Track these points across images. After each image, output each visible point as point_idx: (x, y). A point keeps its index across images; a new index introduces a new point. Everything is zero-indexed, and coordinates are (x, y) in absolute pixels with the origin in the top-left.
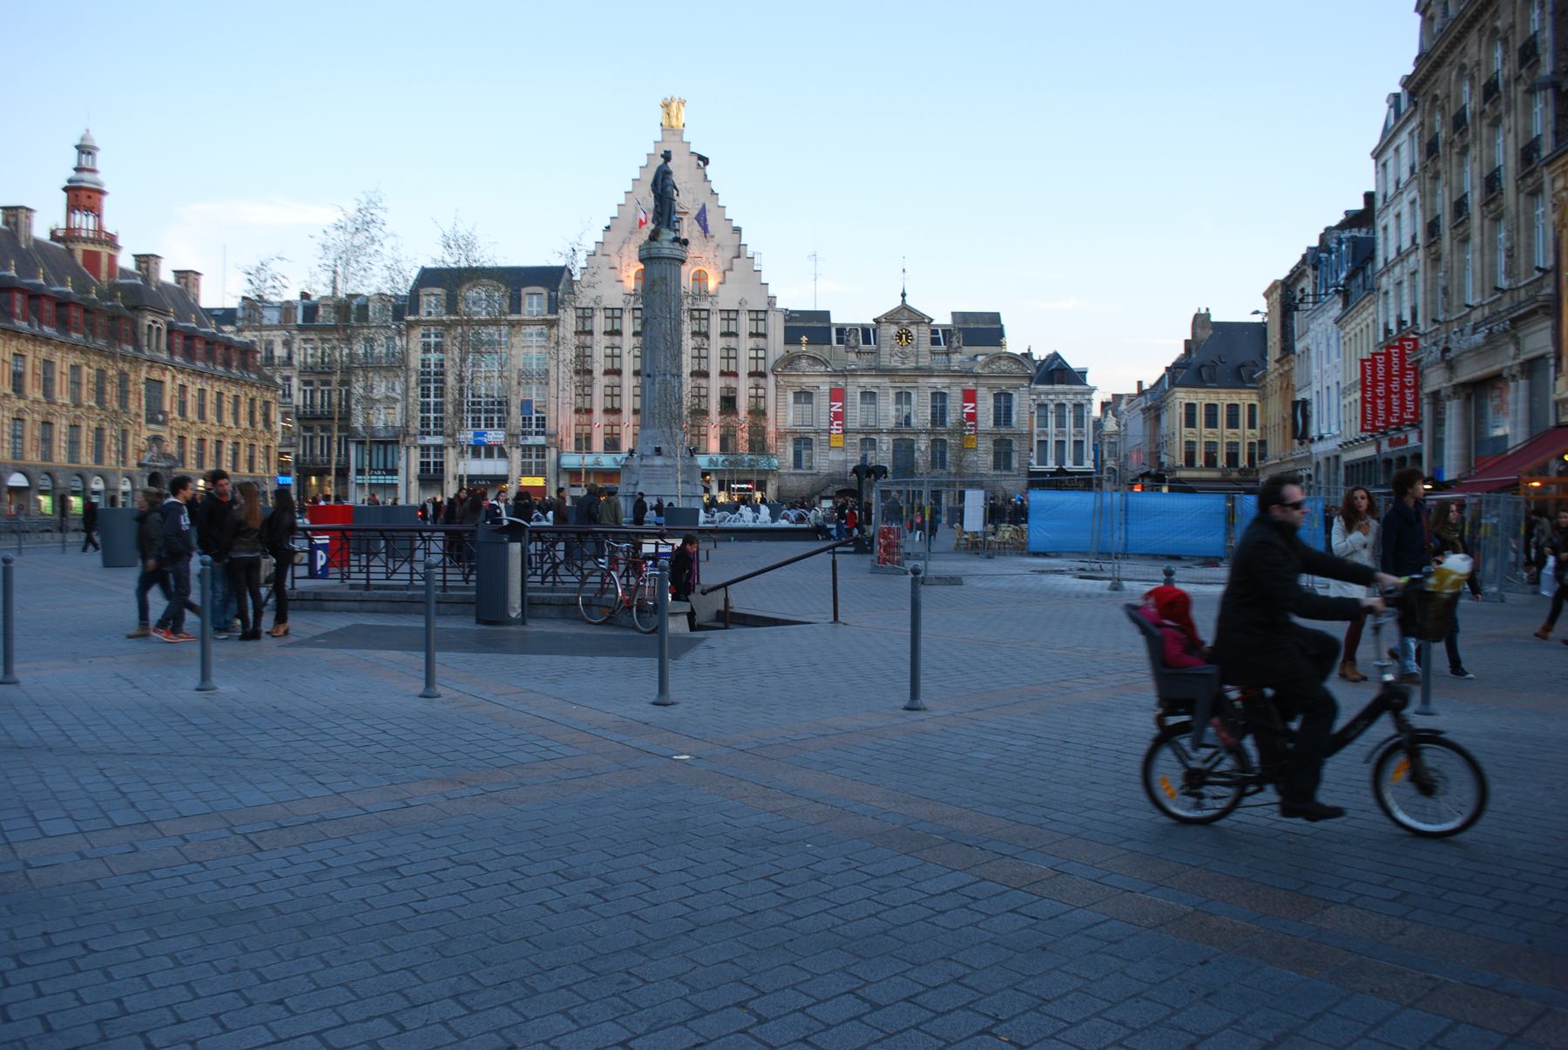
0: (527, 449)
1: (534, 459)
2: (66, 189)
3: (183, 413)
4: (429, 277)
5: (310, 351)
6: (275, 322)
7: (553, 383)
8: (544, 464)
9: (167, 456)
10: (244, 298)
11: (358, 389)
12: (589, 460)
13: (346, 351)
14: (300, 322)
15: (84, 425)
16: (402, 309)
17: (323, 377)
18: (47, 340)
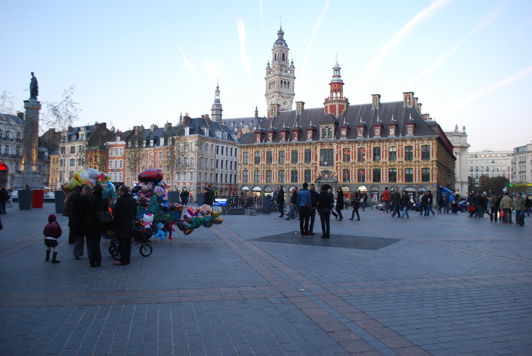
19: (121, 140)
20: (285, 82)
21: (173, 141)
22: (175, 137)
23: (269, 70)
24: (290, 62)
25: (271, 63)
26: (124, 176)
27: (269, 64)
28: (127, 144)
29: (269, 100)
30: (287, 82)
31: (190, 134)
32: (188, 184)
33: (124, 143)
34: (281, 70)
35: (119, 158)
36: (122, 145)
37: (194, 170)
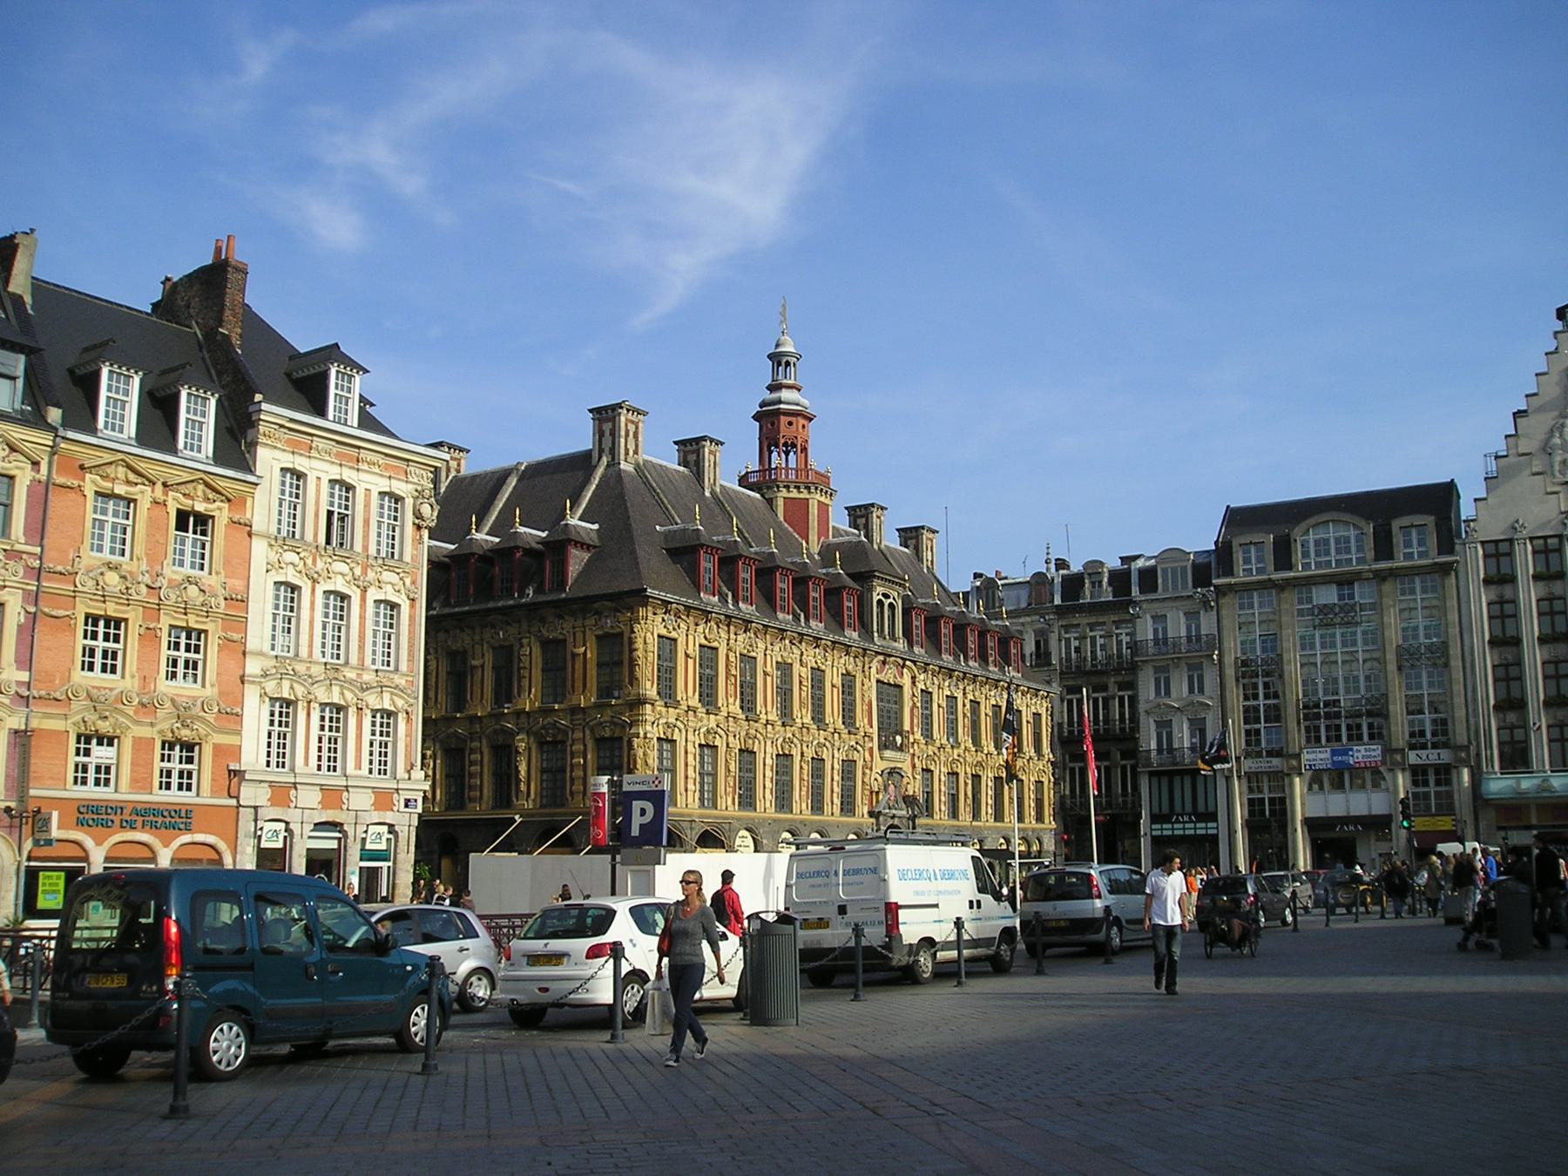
0: (1418, 774)
1: (1432, 788)
2: (757, 417)
3: (928, 734)
4: (1238, 520)
5: (1075, 643)
6: (1023, 605)
7: (1456, 663)
8: (1450, 795)
9: (909, 801)
10: (977, 576)
11: (1147, 690)
12: (1527, 784)
13: (1125, 639)
14: (1058, 601)
15: (796, 752)
16: (1208, 571)
17: (1095, 680)
18: (746, 624)
32: (361, 800)
37: (400, 703)
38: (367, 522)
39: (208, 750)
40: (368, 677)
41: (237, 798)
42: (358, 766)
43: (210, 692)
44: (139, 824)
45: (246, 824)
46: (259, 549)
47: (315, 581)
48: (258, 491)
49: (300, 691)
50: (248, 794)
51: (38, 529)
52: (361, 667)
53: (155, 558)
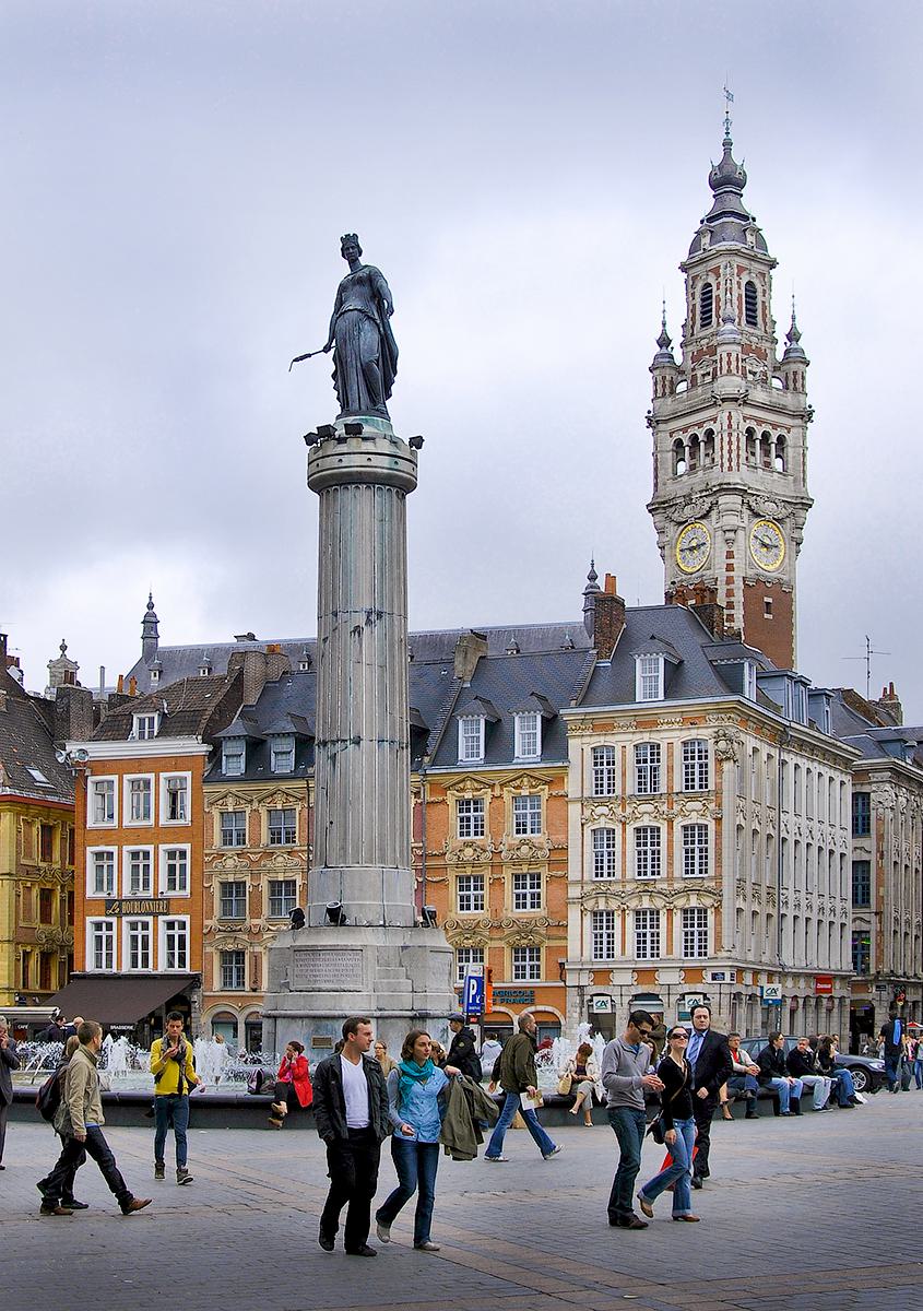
19: (164, 732)
20: (766, 436)
21: (552, 731)
22: (569, 714)
23: (665, 374)
24: (781, 333)
25: (676, 337)
26: (202, 935)
27: (664, 342)
28: (215, 757)
29: (671, 529)
30: (774, 439)
31: (667, 696)
33: (194, 746)
34: (744, 376)
35: (158, 835)
36: (177, 762)
37: (708, 901)
38: (670, 769)
39: (543, 950)
40: (677, 886)
41: (565, 982)
42: (670, 950)
43: (541, 912)
44: (498, 1002)
45: (573, 998)
46: (574, 810)
47: (624, 824)
48: (569, 770)
49: (614, 904)
50: (571, 980)
51: (421, 832)
52: (670, 879)
53: (496, 834)
